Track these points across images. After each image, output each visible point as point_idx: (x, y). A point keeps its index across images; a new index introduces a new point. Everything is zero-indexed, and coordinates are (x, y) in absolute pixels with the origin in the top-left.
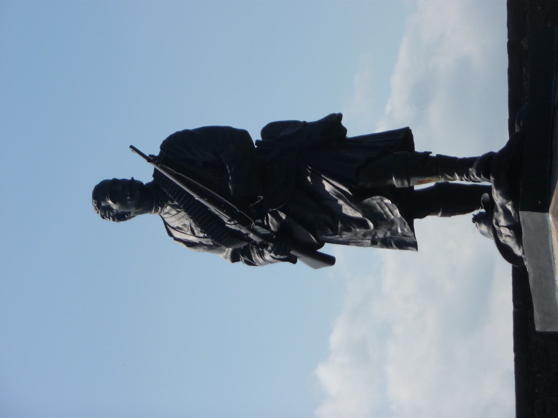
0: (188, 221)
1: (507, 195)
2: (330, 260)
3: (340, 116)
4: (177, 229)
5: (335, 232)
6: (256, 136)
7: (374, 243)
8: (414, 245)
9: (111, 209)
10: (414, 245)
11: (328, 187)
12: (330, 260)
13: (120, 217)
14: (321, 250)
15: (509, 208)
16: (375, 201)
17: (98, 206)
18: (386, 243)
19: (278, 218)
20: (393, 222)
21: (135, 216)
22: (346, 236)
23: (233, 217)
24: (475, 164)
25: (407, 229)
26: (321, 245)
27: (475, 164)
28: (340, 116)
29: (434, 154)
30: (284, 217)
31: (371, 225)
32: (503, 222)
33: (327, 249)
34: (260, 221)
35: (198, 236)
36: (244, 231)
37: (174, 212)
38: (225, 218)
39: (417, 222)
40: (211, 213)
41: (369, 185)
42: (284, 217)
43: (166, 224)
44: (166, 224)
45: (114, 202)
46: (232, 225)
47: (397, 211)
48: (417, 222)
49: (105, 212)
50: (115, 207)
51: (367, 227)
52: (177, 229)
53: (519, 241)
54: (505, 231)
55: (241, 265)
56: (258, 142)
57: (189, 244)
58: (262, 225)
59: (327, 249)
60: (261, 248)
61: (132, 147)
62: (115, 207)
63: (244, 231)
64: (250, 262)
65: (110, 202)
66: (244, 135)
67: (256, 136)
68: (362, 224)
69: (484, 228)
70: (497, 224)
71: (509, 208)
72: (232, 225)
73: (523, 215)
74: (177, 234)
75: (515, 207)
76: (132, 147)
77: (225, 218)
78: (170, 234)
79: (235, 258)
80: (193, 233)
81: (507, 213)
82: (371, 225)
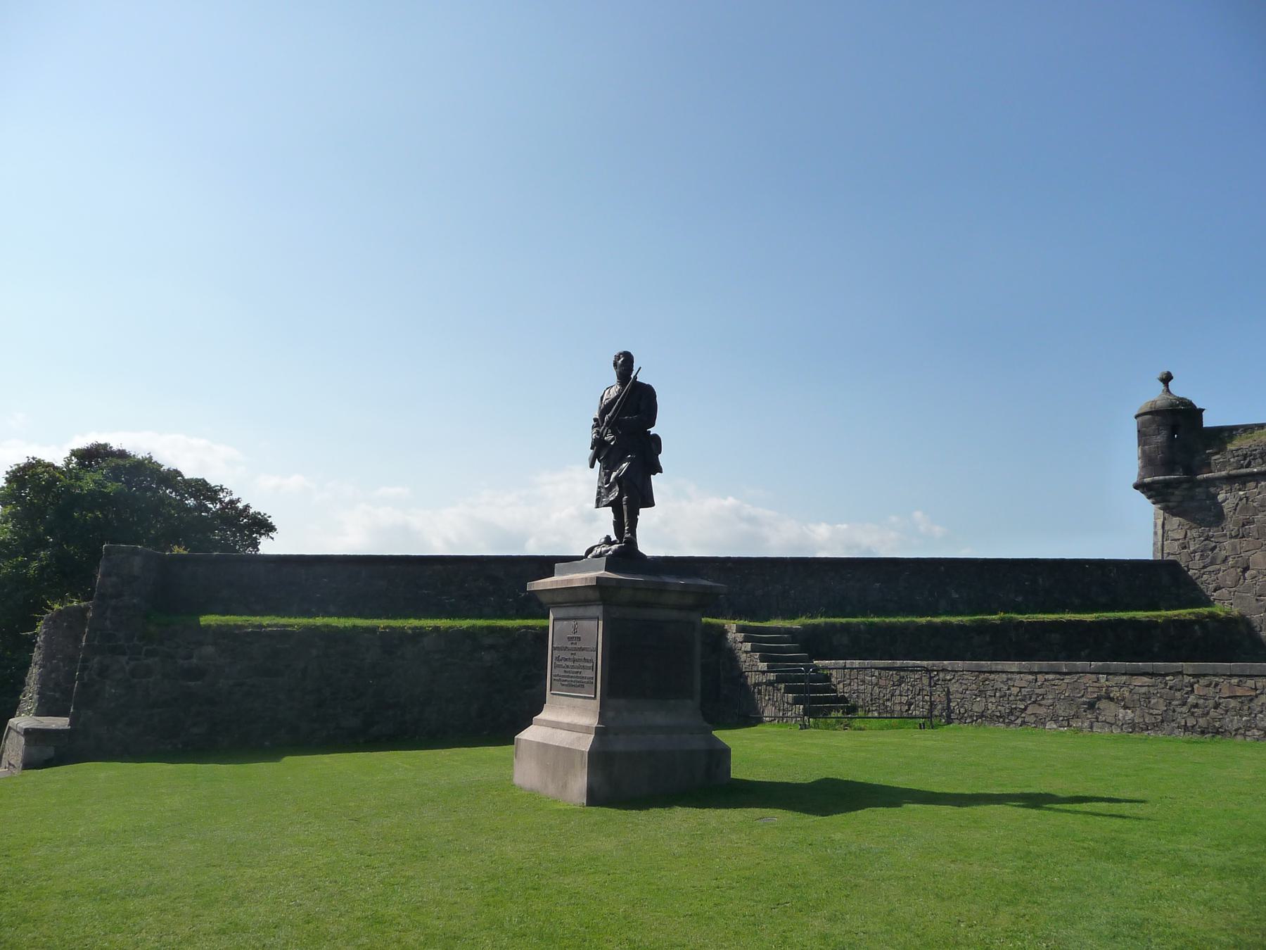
0: (612, 397)
1: (615, 552)
2: (592, 466)
3: (661, 472)
4: (609, 391)
5: (605, 469)
6: (653, 431)
7: (599, 487)
8: (597, 507)
9: (619, 360)
10: (597, 507)
11: (624, 465)
12: (592, 466)
13: (615, 364)
14: (597, 461)
15: (610, 552)
16: (617, 488)
17: (621, 354)
18: (599, 493)
19: (611, 441)
20: (608, 496)
21: (616, 369)
22: (603, 474)
23: (610, 418)
24: (632, 537)
25: (605, 503)
26: (599, 461)
27: (632, 537)
28: (661, 472)
29: (638, 517)
30: (612, 444)
31: (606, 486)
32: (603, 549)
33: (597, 464)
34: (610, 431)
35: (605, 402)
36: (604, 424)
37: (617, 390)
38: (610, 415)
39: (610, 508)
40: (613, 407)
41: (624, 485)
42: (612, 444)
43: (612, 387)
44: (612, 387)
45: (622, 361)
46: (606, 418)
47: (612, 499)
48: (610, 508)
49: (618, 357)
50: (620, 362)
51: (606, 484)
52: (609, 391)
53: (594, 557)
54: (599, 550)
55: (593, 423)
56: (650, 432)
57: (602, 399)
58: (607, 434)
59: (597, 464)
60: (598, 432)
61: (640, 368)
62: (620, 362)
63: (604, 424)
64: (593, 427)
65: (622, 359)
66: (652, 425)
67: (653, 431)
68: (607, 482)
69: (603, 540)
70: (603, 547)
71: (610, 552)
72: (606, 418)
73: (604, 559)
74: (607, 391)
75: (610, 555)
76: (640, 368)
77: (610, 415)
78: (607, 389)
79: (595, 420)
80: (606, 399)
81: (607, 551)
82: (606, 486)
